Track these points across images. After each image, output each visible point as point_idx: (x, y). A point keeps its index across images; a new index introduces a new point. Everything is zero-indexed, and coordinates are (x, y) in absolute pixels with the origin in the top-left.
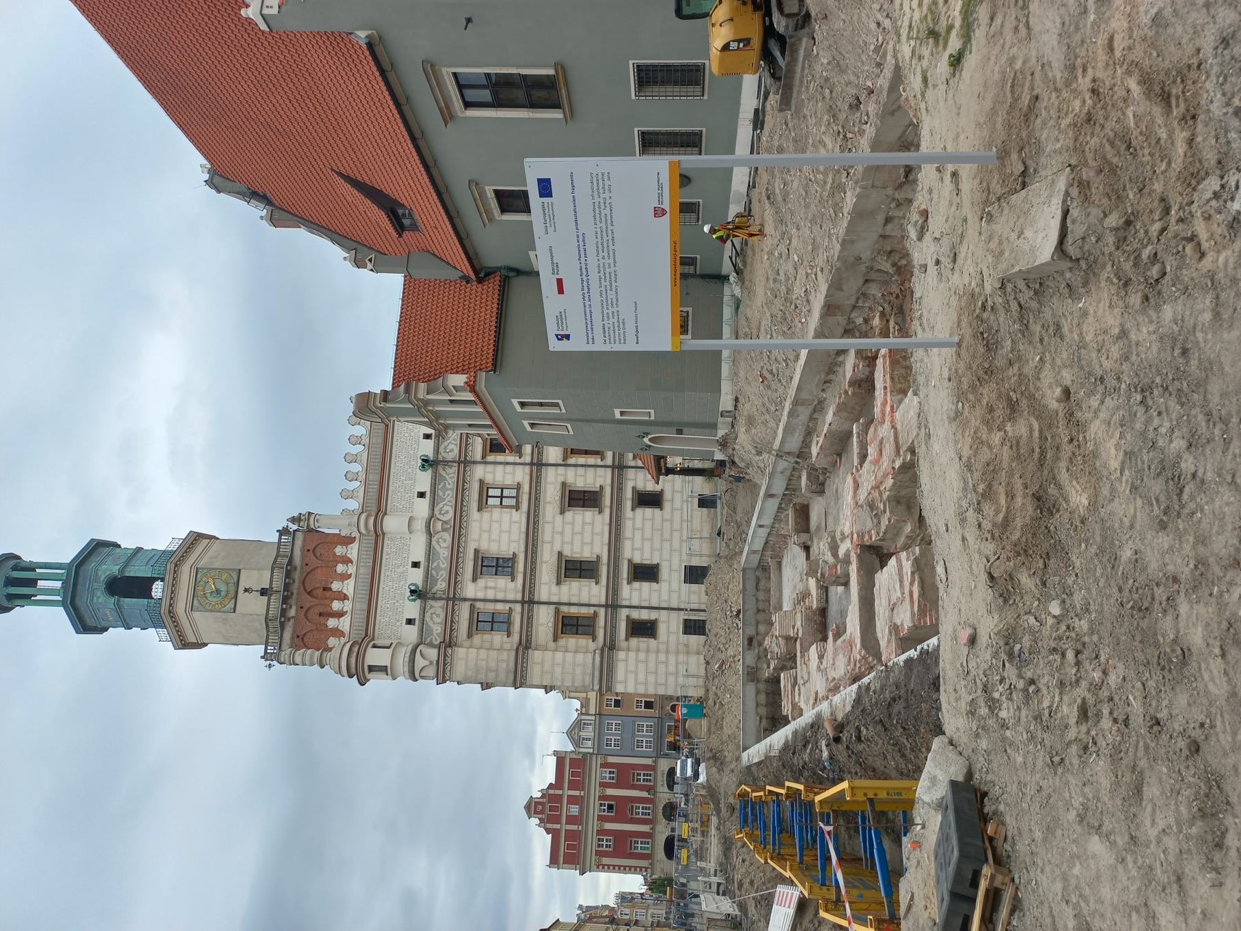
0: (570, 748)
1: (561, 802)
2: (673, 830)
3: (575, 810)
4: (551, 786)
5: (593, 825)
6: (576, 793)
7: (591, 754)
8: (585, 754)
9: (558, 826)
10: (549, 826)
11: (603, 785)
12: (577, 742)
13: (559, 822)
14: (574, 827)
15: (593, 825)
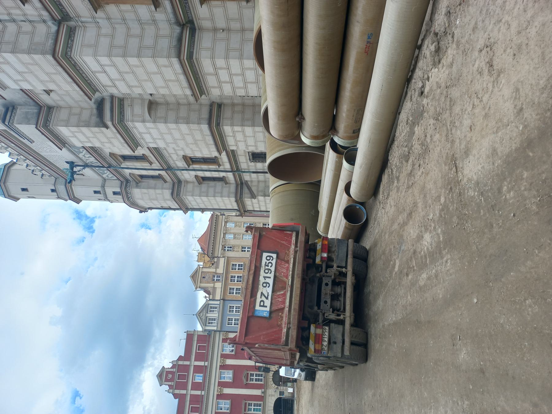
0: (199, 328)
1: (188, 371)
2: (281, 393)
3: (199, 379)
4: (180, 358)
5: (214, 390)
6: (201, 363)
7: (215, 331)
8: (210, 331)
9: (184, 392)
10: (177, 392)
11: (225, 356)
12: (205, 322)
13: (185, 388)
14: (198, 393)
15: (214, 390)
